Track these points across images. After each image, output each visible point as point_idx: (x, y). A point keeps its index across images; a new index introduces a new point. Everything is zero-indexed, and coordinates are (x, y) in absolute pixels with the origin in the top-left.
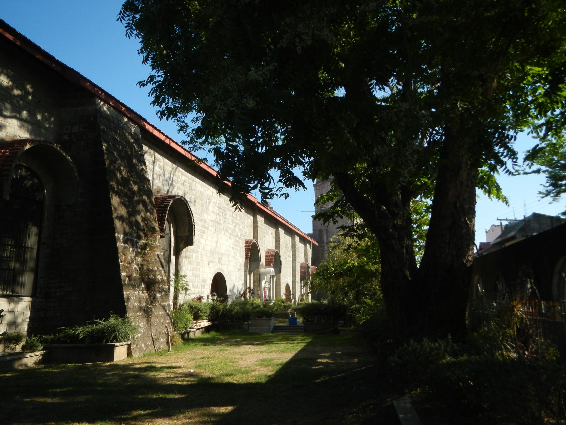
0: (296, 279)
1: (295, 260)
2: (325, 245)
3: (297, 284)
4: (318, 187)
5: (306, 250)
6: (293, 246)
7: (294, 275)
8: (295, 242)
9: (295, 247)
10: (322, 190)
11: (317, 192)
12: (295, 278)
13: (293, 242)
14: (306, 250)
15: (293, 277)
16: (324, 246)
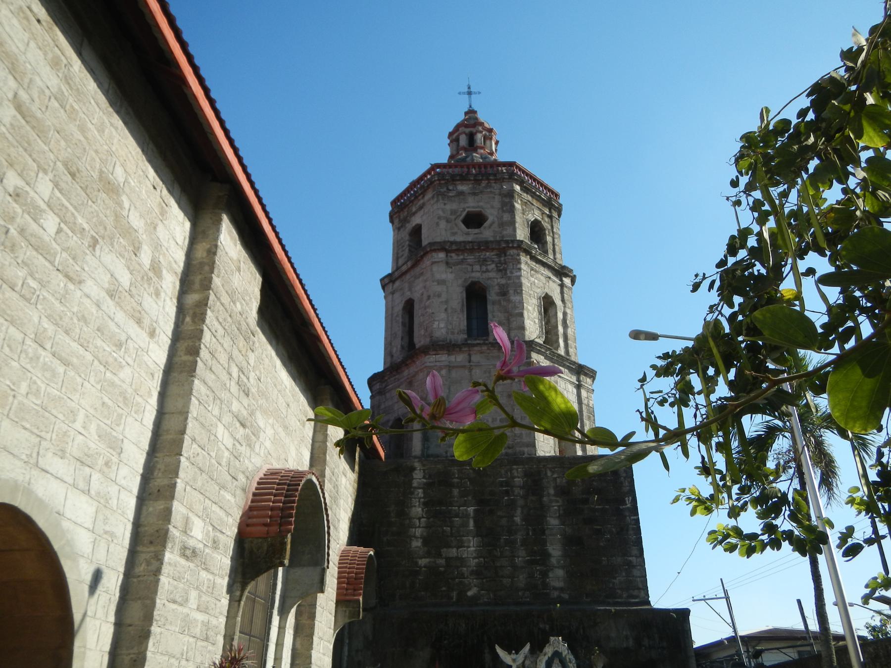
0: (167, 514)
1: (192, 369)
2: (417, 465)
3: (170, 556)
4: (397, 283)
5: (320, 437)
6: (197, 279)
7: (160, 481)
8: (212, 251)
9: (207, 285)
10: (410, 290)
11: (393, 300)
12: (160, 505)
13: (200, 252)
14: (320, 437)
15: (143, 498)
16: (413, 469)
